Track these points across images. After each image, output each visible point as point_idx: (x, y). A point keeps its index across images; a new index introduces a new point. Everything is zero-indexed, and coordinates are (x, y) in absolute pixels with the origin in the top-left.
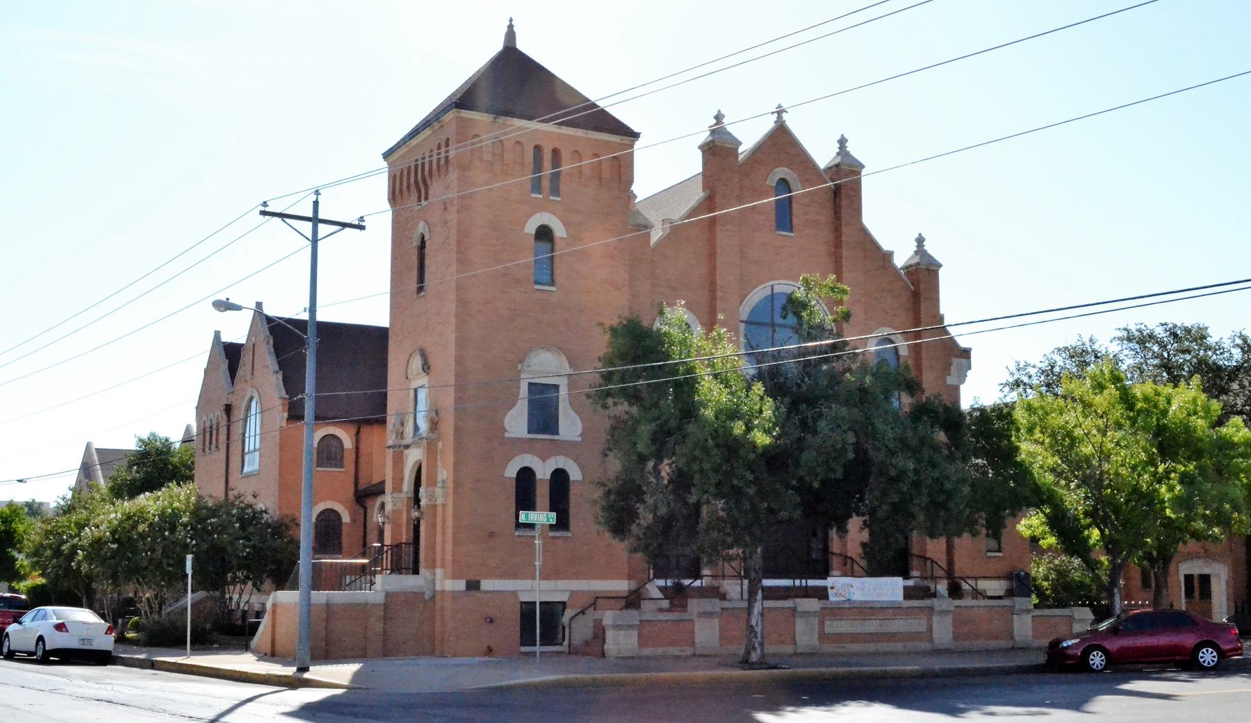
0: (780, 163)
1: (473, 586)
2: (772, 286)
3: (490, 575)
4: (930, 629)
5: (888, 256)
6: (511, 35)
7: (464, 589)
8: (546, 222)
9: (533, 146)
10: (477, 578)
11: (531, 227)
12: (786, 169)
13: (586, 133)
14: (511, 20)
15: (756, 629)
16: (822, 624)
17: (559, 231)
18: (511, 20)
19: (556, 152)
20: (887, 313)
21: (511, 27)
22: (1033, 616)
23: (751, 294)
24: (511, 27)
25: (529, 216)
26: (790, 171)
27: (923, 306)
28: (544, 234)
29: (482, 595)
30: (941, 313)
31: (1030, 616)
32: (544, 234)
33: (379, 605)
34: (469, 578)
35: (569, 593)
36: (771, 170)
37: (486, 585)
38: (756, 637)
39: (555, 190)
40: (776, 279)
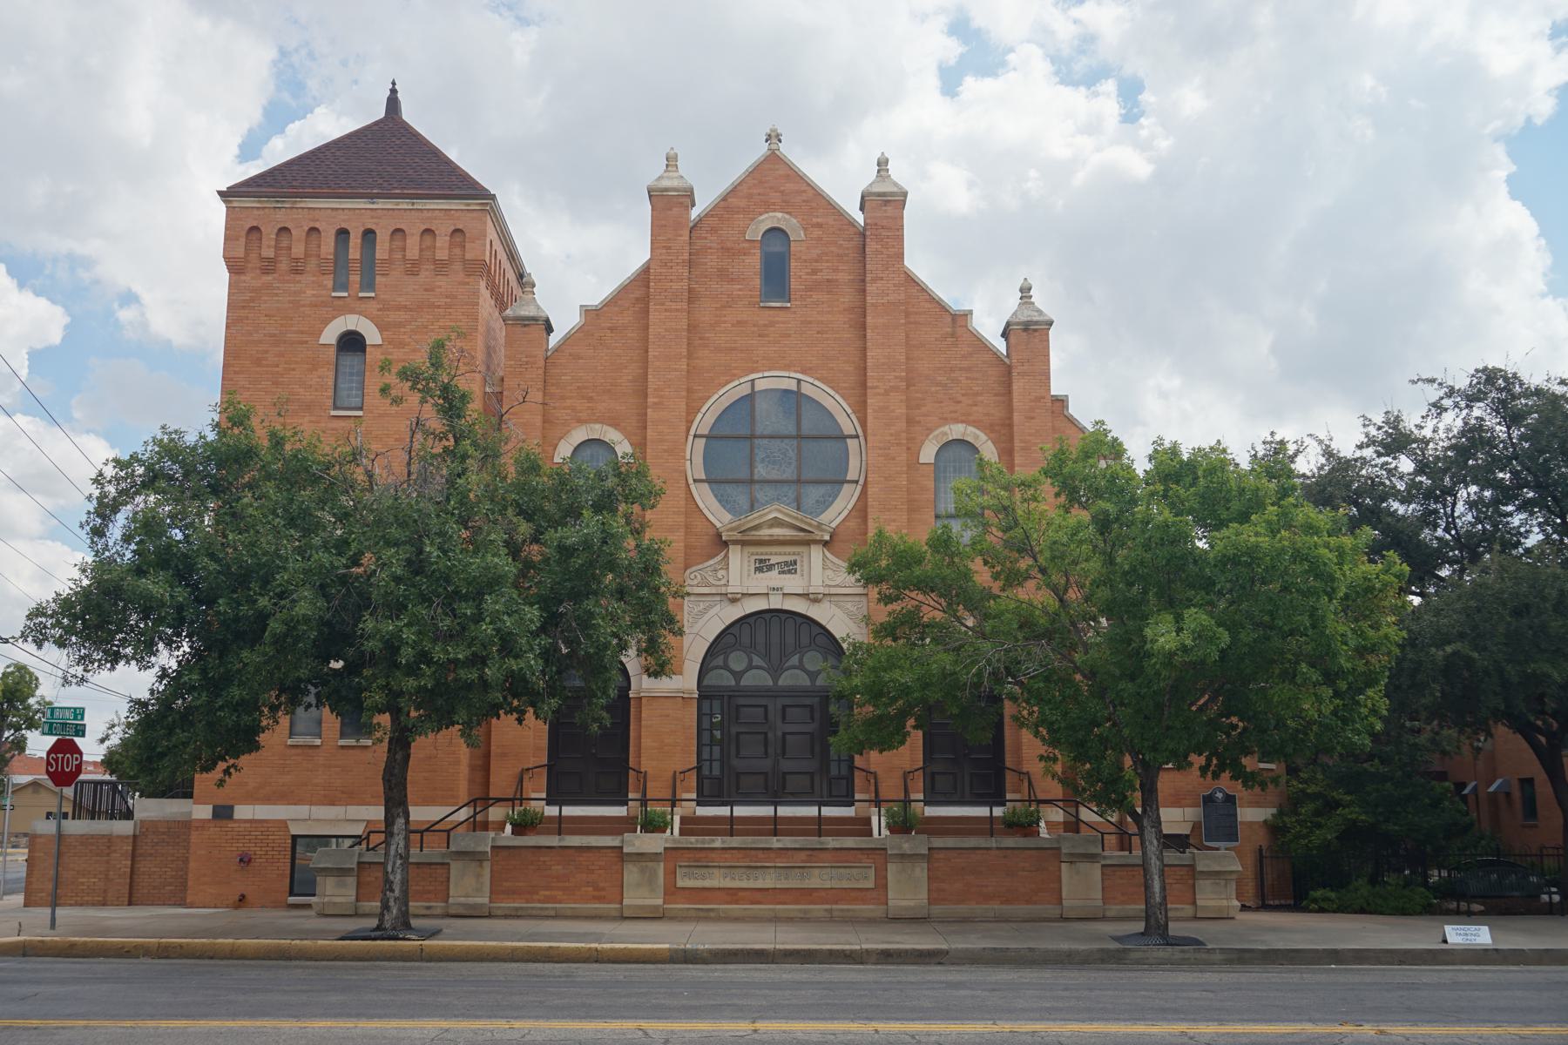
0: (768, 207)
1: (223, 813)
2: (753, 380)
3: (252, 798)
4: (882, 885)
5: (960, 320)
6: (393, 103)
7: (210, 817)
8: (351, 327)
9: (334, 232)
10: (230, 803)
11: (330, 335)
12: (779, 215)
13: (413, 204)
14: (394, 83)
15: (391, 877)
16: (671, 874)
17: (372, 336)
18: (394, 83)
19: (369, 234)
20: (959, 402)
21: (394, 91)
22: (1103, 866)
23: (716, 396)
24: (394, 91)
25: (326, 322)
26: (787, 216)
27: (1018, 386)
28: (352, 343)
29: (237, 825)
30: (1056, 389)
31: (1099, 865)
32: (352, 343)
33: (127, 837)
34: (220, 802)
35: (365, 824)
36: (752, 219)
37: (243, 812)
38: (392, 891)
39: (369, 284)
40: (758, 372)
